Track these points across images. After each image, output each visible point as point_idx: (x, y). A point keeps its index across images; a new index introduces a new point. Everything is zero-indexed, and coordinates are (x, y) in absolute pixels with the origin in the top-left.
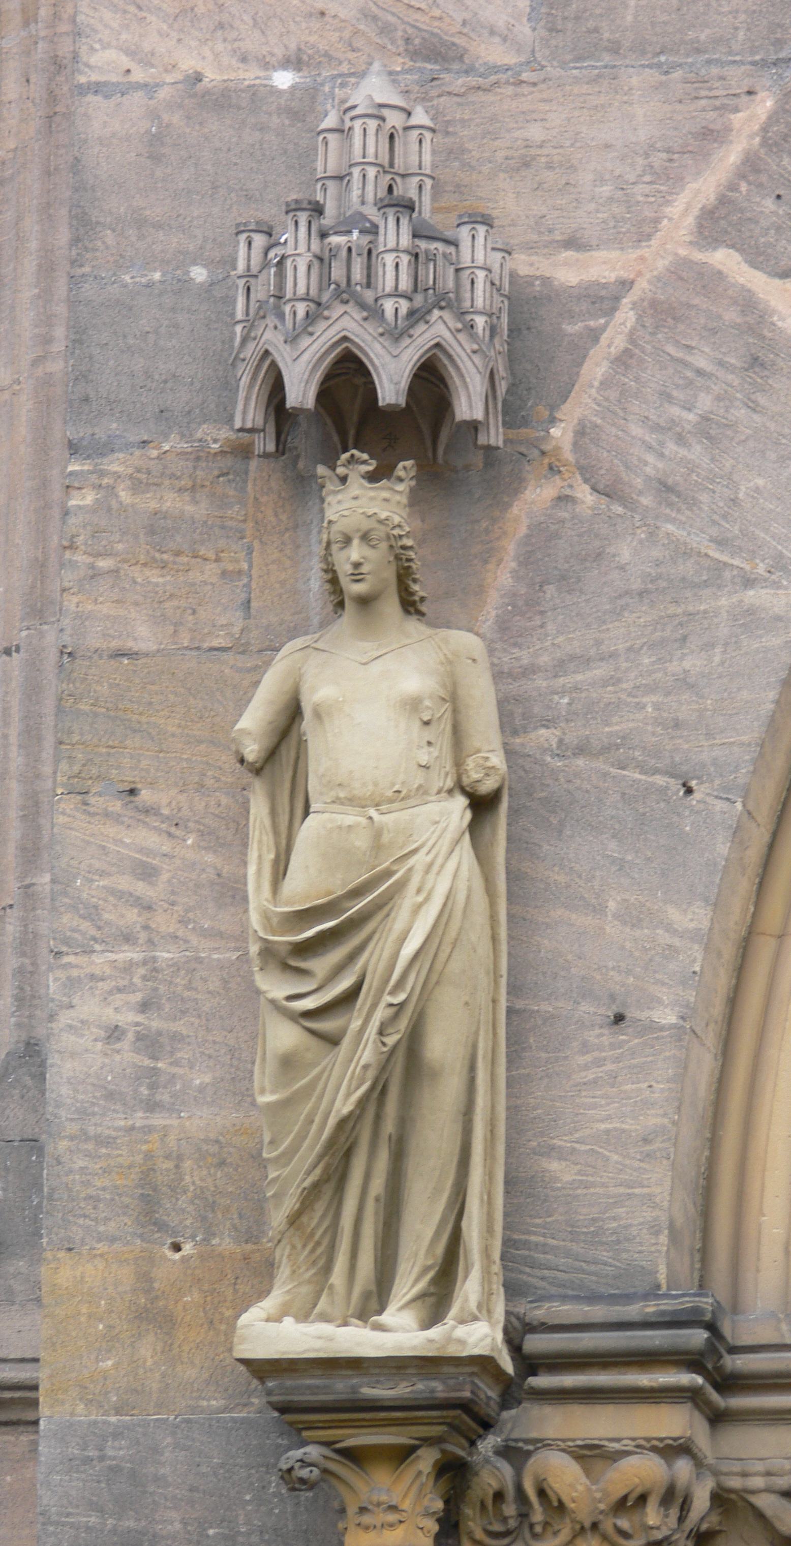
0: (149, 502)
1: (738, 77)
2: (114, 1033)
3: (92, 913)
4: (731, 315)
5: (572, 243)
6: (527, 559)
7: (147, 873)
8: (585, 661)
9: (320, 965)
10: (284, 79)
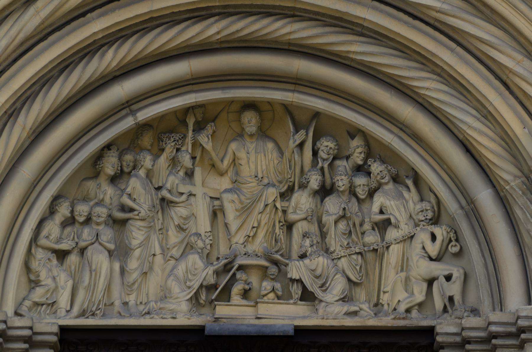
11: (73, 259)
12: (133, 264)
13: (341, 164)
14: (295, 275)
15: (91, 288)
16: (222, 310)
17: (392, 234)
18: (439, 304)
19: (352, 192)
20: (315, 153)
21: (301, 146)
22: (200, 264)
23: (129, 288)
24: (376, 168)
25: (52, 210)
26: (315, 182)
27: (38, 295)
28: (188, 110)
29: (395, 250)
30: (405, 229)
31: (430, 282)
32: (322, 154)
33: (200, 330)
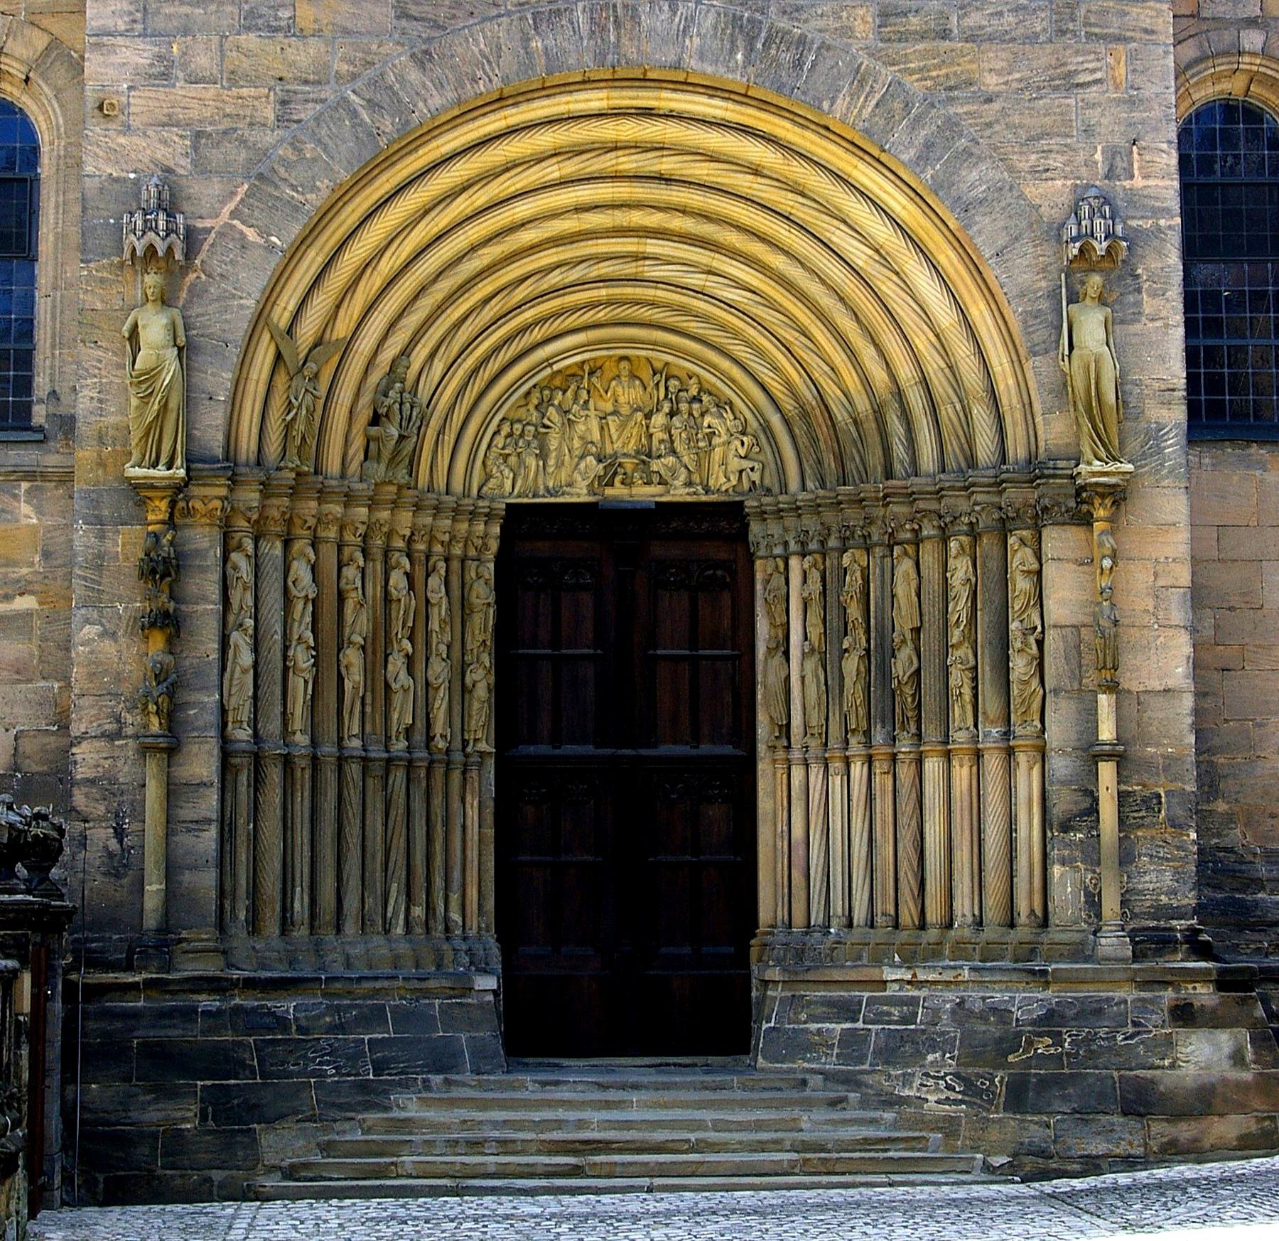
0: (100, 275)
1: (240, 180)
2: (92, 398)
3: (87, 370)
4: (237, 236)
5: (201, 217)
6: (189, 291)
7: (100, 361)
8: (203, 315)
9: (144, 386)
10: (132, 176)
11: (513, 460)
12: (551, 462)
15: (526, 478)
16: (609, 491)
17: (716, 441)
18: (746, 485)
19: (691, 414)
20: (667, 388)
21: (657, 384)
22: (595, 462)
24: (705, 398)
26: (666, 407)
29: (718, 451)
30: (725, 438)
31: (741, 472)
32: (671, 389)
33: (595, 504)
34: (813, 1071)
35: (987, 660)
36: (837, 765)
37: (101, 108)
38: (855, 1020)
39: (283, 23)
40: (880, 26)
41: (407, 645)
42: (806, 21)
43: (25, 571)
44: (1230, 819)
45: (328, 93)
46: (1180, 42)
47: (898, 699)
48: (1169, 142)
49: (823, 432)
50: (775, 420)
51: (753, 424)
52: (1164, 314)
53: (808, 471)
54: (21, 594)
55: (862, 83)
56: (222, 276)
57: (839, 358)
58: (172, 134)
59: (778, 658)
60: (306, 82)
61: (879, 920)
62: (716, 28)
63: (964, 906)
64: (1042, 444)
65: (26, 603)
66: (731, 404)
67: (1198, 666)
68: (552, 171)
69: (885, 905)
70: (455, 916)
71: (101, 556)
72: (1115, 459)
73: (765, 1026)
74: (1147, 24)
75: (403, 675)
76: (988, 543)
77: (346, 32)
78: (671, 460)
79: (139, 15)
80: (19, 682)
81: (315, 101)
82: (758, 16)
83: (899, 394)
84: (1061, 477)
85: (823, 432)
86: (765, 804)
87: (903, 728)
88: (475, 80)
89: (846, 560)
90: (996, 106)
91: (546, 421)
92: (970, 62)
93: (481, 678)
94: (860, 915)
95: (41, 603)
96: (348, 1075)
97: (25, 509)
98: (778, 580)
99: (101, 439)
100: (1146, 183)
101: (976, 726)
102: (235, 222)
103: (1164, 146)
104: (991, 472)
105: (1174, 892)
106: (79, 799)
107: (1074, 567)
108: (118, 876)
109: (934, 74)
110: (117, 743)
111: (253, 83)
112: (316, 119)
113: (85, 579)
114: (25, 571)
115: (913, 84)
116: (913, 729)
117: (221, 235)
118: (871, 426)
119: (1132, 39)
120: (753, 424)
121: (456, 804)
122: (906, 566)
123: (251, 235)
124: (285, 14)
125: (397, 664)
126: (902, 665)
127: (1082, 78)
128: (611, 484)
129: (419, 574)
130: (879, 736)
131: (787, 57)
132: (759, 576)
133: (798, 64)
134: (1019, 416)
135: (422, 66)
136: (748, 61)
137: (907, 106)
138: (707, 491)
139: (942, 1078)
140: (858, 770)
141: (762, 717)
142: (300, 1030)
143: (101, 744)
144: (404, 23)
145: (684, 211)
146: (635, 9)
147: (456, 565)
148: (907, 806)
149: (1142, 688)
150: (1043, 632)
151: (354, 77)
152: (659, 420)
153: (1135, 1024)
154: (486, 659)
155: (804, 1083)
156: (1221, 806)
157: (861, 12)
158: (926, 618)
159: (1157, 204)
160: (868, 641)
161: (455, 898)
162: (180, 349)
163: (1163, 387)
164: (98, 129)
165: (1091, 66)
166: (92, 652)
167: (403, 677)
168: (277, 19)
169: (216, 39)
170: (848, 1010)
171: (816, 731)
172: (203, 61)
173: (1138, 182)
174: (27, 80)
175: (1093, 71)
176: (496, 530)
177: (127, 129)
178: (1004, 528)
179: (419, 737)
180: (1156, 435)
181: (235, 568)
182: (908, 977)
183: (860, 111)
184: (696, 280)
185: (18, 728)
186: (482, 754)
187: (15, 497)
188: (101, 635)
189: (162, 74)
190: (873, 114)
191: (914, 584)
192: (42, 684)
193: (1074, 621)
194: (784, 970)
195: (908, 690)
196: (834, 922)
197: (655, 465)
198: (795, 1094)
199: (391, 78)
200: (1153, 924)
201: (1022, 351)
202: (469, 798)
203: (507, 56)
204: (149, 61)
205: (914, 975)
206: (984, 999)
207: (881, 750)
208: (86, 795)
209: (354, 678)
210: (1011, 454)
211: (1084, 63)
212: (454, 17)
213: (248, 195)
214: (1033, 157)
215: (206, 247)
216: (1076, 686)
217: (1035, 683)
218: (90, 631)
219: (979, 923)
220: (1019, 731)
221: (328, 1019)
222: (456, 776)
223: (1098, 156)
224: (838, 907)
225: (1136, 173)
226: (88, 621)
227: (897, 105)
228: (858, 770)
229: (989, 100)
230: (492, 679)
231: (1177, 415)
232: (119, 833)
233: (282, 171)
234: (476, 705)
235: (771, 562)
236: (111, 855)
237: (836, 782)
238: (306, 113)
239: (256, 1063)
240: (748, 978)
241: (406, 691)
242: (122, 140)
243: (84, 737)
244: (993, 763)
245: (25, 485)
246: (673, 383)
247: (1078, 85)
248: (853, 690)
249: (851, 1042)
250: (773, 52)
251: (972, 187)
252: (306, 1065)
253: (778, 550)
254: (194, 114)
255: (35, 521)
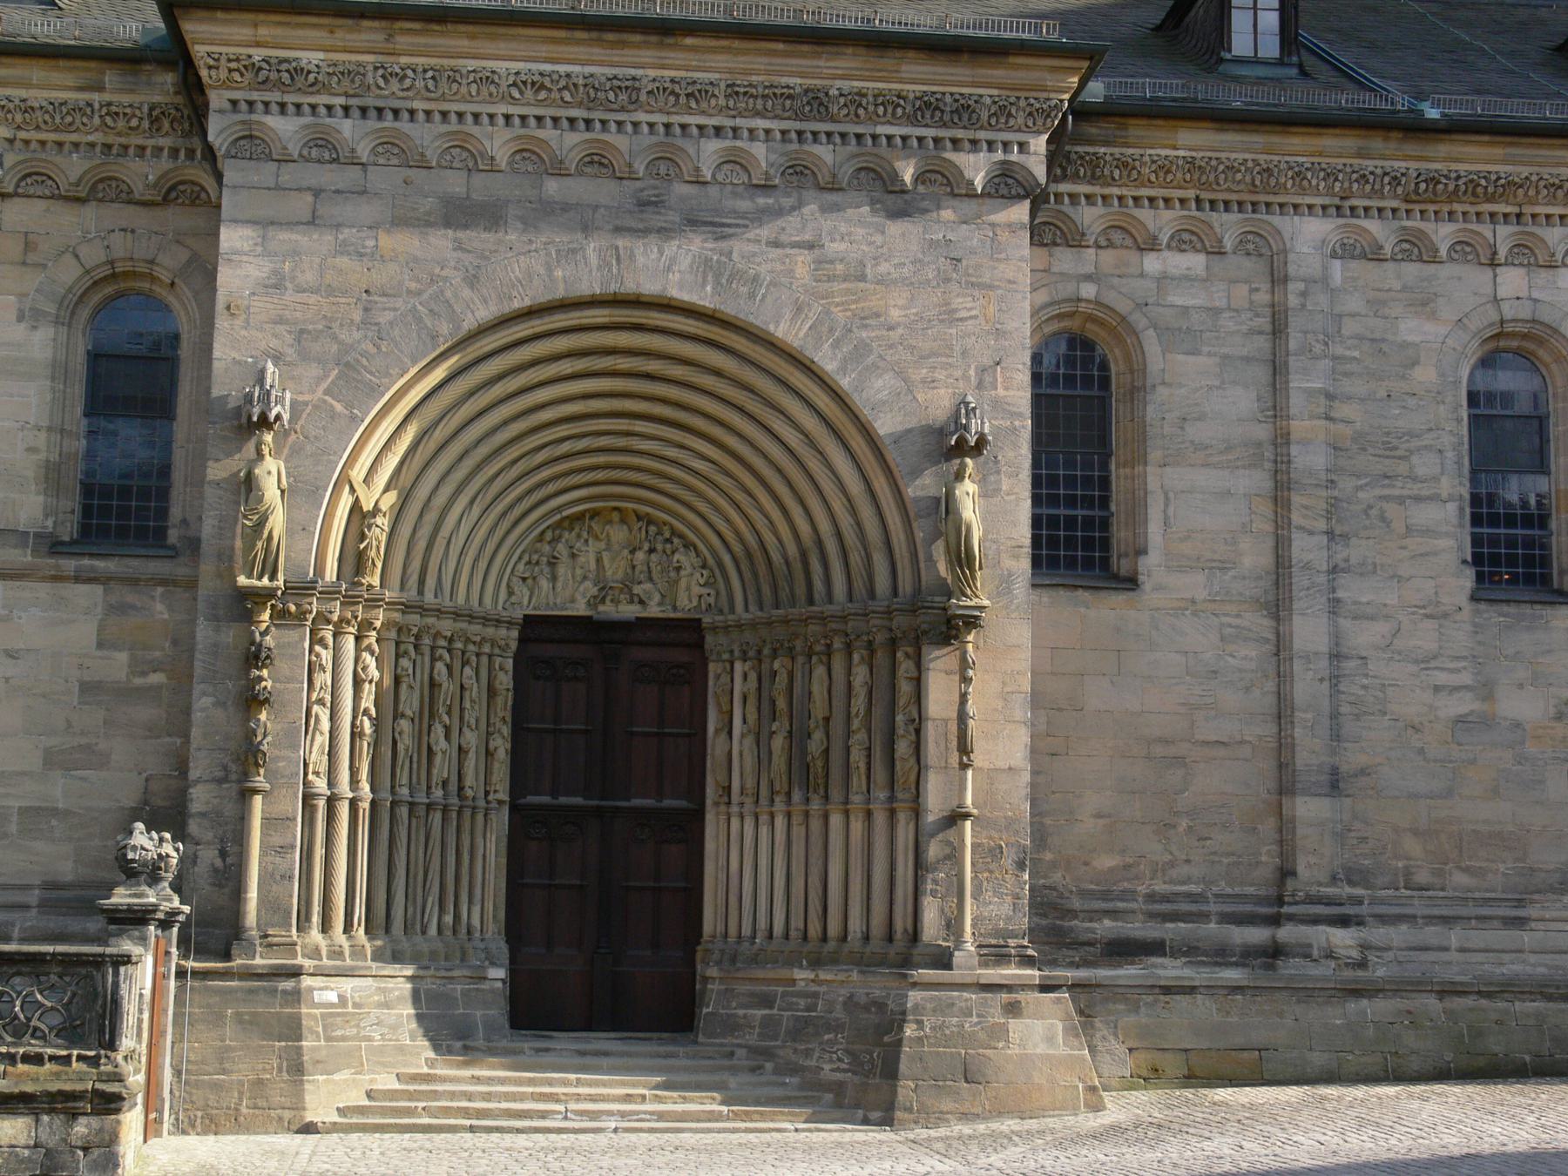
7: (220, 498)
11: (530, 581)
12: (559, 585)
13: (660, 538)
14: (635, 592)
16: (601, 608)
17: (683, 573)
19: (664, 552)
23: (555, 595)
24: (676, 541)
25: (520, 558)
26: (646, 546)
27: (513, 599)
28: (585, 511)
29: (683, 583)
30: (689, 570)
31: (700, 597)
33: (589, 618)
34: (739, 1046)
35: (878, 742)
36: (764, 818)
37: (228, 308)
38: (771, 1007)
39: (368, 251)
40: (815, 270)
41: (446, 718)
42: (759, 264)
43: (157, 654)
44: (1054, 865)
45: (399, 303)
46: (1035, 290)
47: (812, 770)
48: (1024, 364)
49: (762, 569)
50: (727, 559)
51: (711, 561)
52: (1016, 490)
53: (750, 597)
54: (154, 671)
55: (799, 310)
56: (316, 437)
57: (776, 514)
58: (281, 329)
59: (724, 736)
60: (384, 295)
61: (793, 933)
62: (691, 267)
63: (856, 926)
64: (923, 583)
65: (157, 678)
66: (695, 548)
67: (1034, 751)
68: (566, 367)
69: (797, 922)
70: (476, 922)
71: (216, 645)
72: (977, 597)
73: (705, 1010)
74: (1010, 275)
75: (442, 739)
76: (881, 657)
77: (416, 259)
78: (648, 586)
79: (260, 240)
80: (151, 737)
81: (389, 309)
82: (723, 259)
83: (819, 543)
84: (939, 608)
85: (762, 569)
86: (710, 846)
87: (815, 791)
88: (511, 299)
89: (776, 665)
90: (900, 331)
91: (555, 554)
92: (881, 299)
93: (501, 746)
94: (778, 928)
95: (169, 678)
96: (390, 1040)
97: (159, 607)
98: (725, 679)
99: (219, 556)
100: (1005, 393)
101: (869, 791)
102: (326, 398)
103: (1020, 367)
104: (886, 603)
105: (1009, 919)
106: (193, 827)
107: (943, 675)
108: (220, 886)
109: (854, 307)
110: (224, 786)
111: (344, 293)
112: (391, 323)
113: (204, 662)
114: (157, 654)
115: (840, 316)
116: (822, 791)
117: (316, 407)
118: (797, 566)
119: (998, 287)
120: (711, 561)
121: (479, 841)
122: (820, 672)
123: (339, 407)
124: (371, 243)
125: (439, 730)
126: (815, 745)
127: (964, 314)
128: (603, 601)
129: (457, 665)
130: (797, 796)
131: (744, 290)
132: (711, 676)
133: (752, 296)
134: (907, 562)
135: (472, 287)
136: (715, 292)
137: (831, 330)
138: (675, 608)
139: (835, 1053)
140: (780, 822)
141: (709, 780)
142: (355, 1005)
143: (213, 786)
144: (459, 254)
145: (664, 401)
146: (632, 252)
147: (485, 659)
148: (816, 850)
149: (992, 766)
150: (920, 723)
151: (419, 293)
152: (640, 556)
153: (978, 1016)
154: (506, 730)
155: (732, 1054)
156: (1048, 856)
157: (800, 259)
158: (834, 710)
159: (1015, 409)
160: (791, 726)
161: (476, 910)
162: (283, 492)
163: (1014, 544)
164: (226, 324)
165: (969, 305)
166: (208, 717)
167: (443, 744)
168: (364, 247)
169: (318, 260)
170: (766, 1001)
171: (750, 792)
172: (309, 277)
173: (1001, 392)
174: (173, 284)
175: (970, 309)
176: (515, 634)
177: (246, 327)
178: (893, 644)
179: (453, 787)
180: (1007, 579)
181: (318, 655)
182: (812, 976)
183: (796, 334)
184: (672, 452)
185: (149, 772)
186: (500, 802)
187: (153, 597)
188: (218, 704)
189: (276, 284)
190: (807, 335)
191: (826, 684)
192: (168, 739)
193: (944, 716)
194: (721, 969)
195: (819, 763)
196: (759, 934)
197: (637, 590)
198: (726, 1062)
199: (448, 294)
200: (994, 942)
201: (912, 515)
202: (488, 835)
203: (536, 281)
204: (265, 275)
205: (817, 976)
206: (868, 994)
207: (798, 809)
208: (199, 825)
209: (406, 742)
210: (900, 590)
211: (963, 303)
212: (496, 251)
213: (338, 377)
214: (924, 371)
215: (304, 416)
216: (943, 765)
217: (912, 761)
218: (207, 701)
219: (867, 938)
220: (900, 795)
221: (376, 998)
222: (480, 818)
223: (972, 372)
224: (762, 923)
225: (999, 385)
226: (204, 694)
227: (825, 329)
228: (780, 822)
229: (891, 328)
230: (509, 746)
231: (1025, 564)
232: (223, 854)
233: (364, 361)
234: (496, 765)
235: (720, 664)
236: (216, 870)
237: (764, 831)
238: (385, 318)
239: (320, 1029)
240: (694, 974)
241: (444, 753)
242: (243, 332)
243: (197, 781)
244: (880, 819)
245: (160, 590)
246: (653, 529)
247: (961, 320)
248: (779, 761)
249: (769, 1026)
250: (734, 286)
251: (879, 391)
252: (358, 1033)
253: (726, 656)
254: (298, 314)
255: (166, 616)
